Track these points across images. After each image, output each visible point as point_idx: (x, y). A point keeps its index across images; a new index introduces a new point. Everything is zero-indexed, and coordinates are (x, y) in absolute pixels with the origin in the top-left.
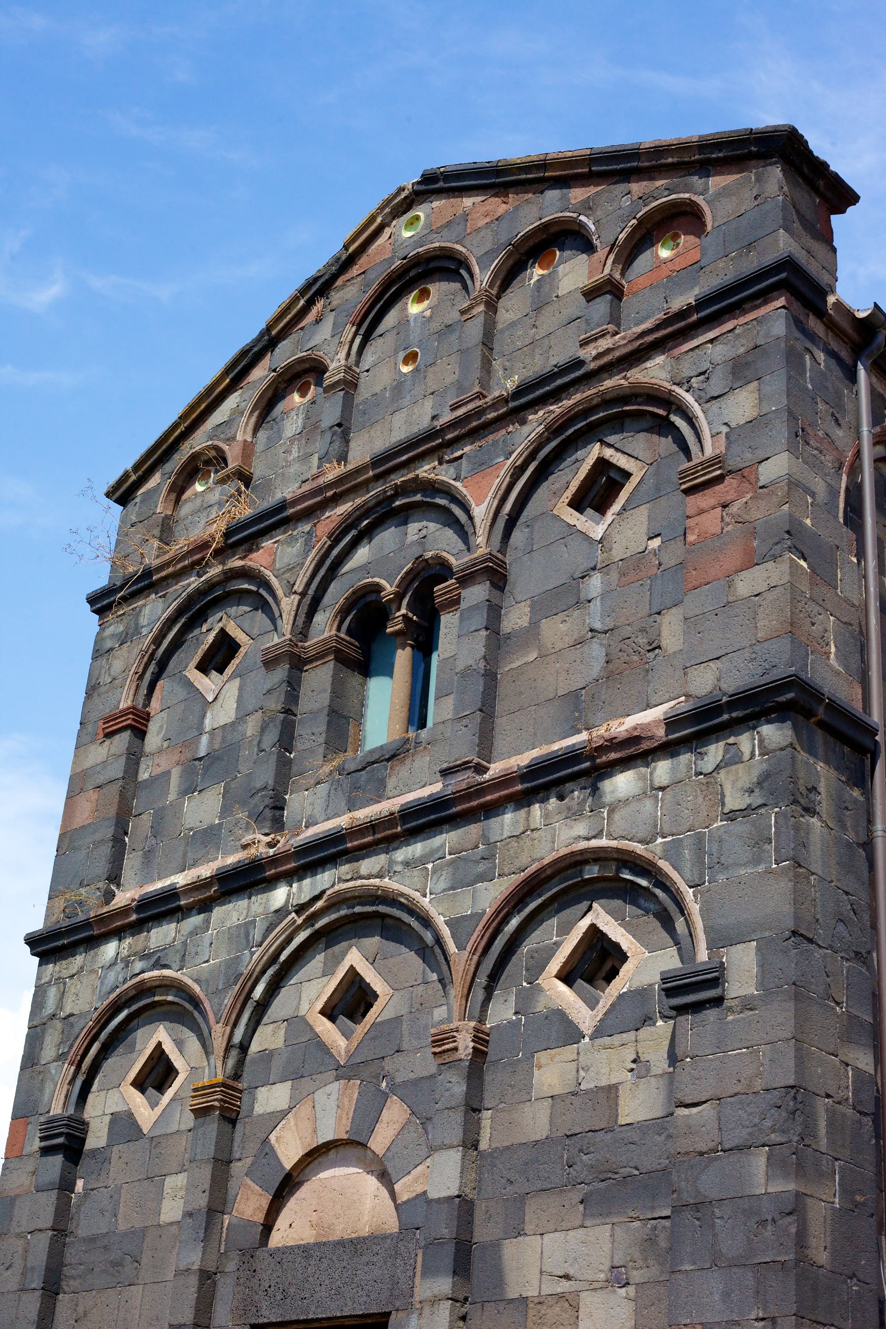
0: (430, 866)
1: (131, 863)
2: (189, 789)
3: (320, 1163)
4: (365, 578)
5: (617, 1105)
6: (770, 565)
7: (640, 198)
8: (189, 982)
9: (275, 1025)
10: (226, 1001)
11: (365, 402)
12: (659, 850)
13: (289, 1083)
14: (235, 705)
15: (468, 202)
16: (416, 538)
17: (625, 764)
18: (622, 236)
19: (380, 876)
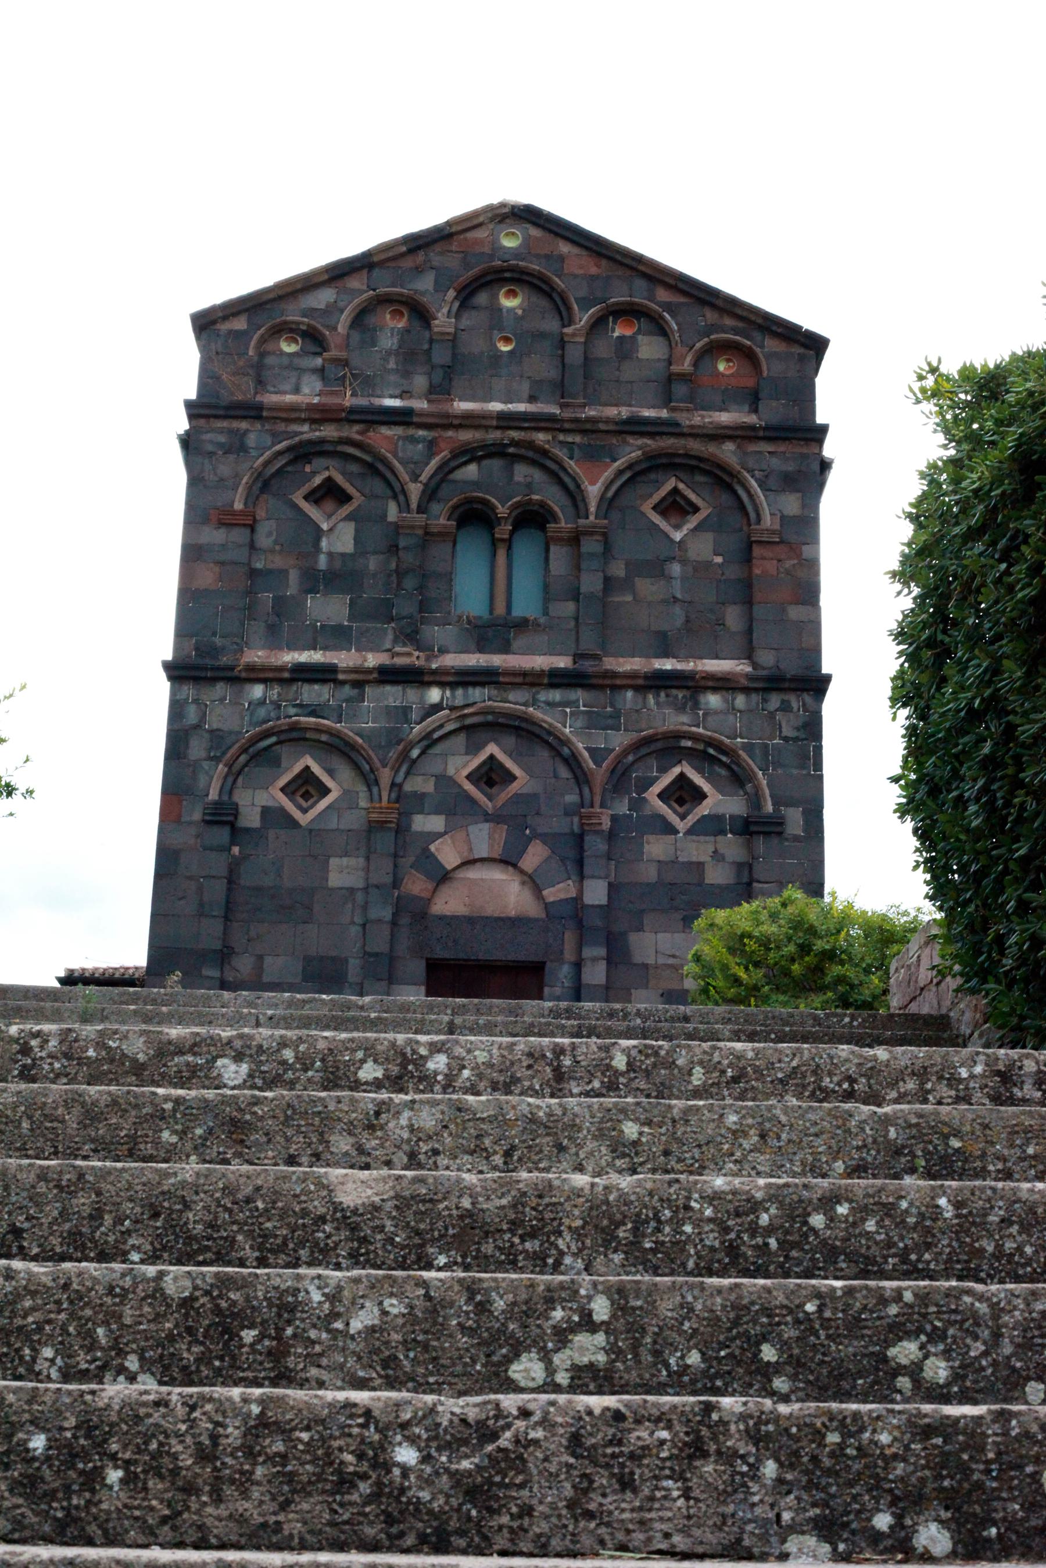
2: (314, 590)
8: (351, 734)
16: (521, 479)
17: (715, 690)
18: (698, 345)
19: (525, 704)
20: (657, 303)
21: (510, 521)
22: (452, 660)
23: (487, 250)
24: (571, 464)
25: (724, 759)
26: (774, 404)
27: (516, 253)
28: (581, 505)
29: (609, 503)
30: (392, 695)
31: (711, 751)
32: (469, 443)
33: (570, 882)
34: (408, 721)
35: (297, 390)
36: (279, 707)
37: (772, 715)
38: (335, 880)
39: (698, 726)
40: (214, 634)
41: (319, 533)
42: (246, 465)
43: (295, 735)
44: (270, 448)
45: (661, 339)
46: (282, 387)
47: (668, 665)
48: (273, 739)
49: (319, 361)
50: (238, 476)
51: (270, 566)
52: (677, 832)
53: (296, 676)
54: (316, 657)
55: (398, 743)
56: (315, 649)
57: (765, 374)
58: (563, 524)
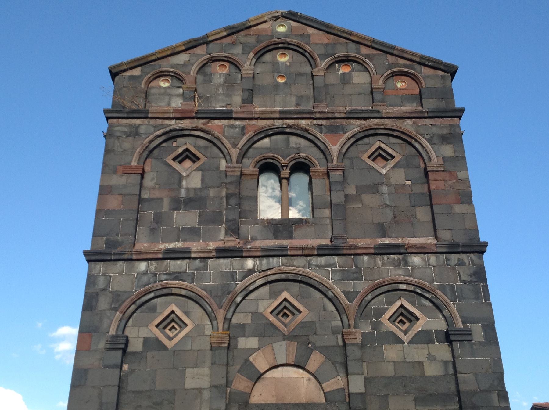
0: (330, 269)
1: (143, 232)
3: (274, 371)
4: (270, 153)
5: (424, 368)
6: (467, 205)
7: (393, 64)
9: (245, 314)
10: (224, 301)
11: (259, 85)
12: (436, 287)
13: (257, 338)
14: (200, 182)
15: (310, 31)
16: (294, 146)
18: (386, 74)
20: (363, 55)
21: (289, 167)
22: (258, 244)
23: (270, 34)
24: (320, 136)
25: (427, 295)
26: (431, 100)
27: (286, 35)
28: (328, 157)
29: (343, 155)
30: (224, 264)
31: (418, 291)
32: (265, 127)
33: (339, 377)
34: (234, 280)
35: (169, 104)
36: (156, 275)
37: (453, 268)
38: (190, 383)
39: (409, 276)
40: (117, 235)
41: (181, 177)
42: (139, 143)
43: (165, 291)
44: (152, 133)
45: (365, 73)
46: (160, 104)
47: (387, 241)
48: (152, 295)
49: (181, 91)
50: (134, 149)
51: (152, 196)
52: (403, 342)
53: (166, 256)
54: (180, 245)
55: (229, 293)
56: (178, 241)
57: (424, 86)
58: (319, 168)
